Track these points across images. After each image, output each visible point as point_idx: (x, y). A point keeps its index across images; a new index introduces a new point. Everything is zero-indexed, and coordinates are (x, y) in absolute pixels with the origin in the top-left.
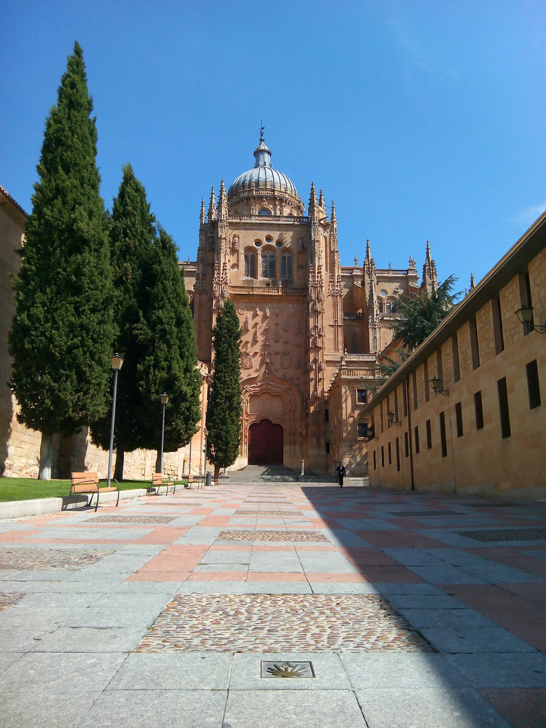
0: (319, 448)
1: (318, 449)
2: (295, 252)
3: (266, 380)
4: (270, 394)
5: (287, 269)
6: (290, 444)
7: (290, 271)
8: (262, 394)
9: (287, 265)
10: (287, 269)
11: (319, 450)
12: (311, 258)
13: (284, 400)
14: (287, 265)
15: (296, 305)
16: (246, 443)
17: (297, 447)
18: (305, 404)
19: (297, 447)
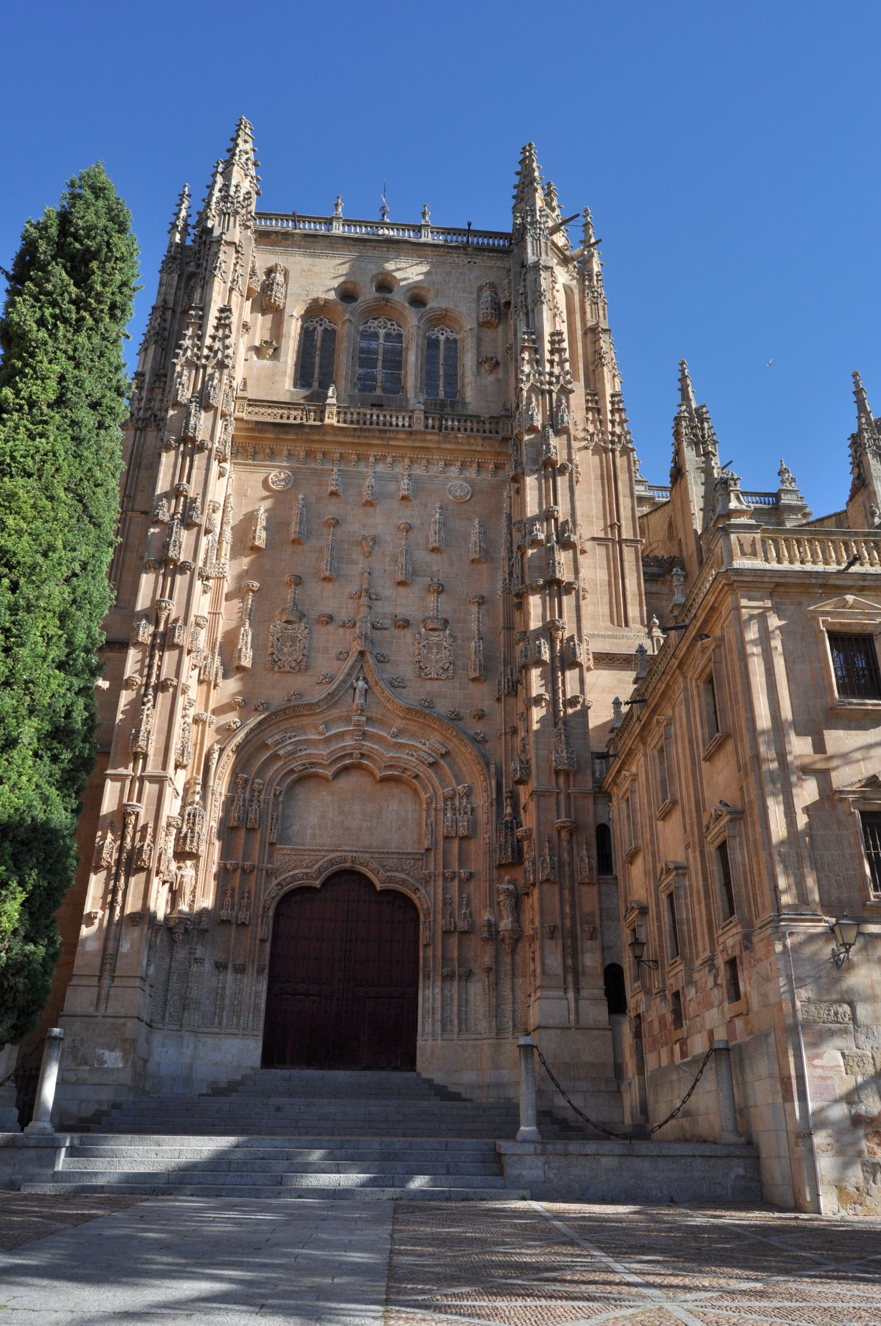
0: (577, 991)
1: (571, 995)
2: (469, 324)
3: (356, 718)
4: (371, 774)
5: (441, 373)
6: (447, 978)
7: (452, 377)
8: (337, 775)
9: (441, 361)
10: (441, 373)
11: (577, 1001)
12: (527, 314)
13: (424, 796)
14: (441, 361)
15: (471, 473)
16: (260, 972)
17: (477, 989)
18: (509, 810)
19: (477, 989)
